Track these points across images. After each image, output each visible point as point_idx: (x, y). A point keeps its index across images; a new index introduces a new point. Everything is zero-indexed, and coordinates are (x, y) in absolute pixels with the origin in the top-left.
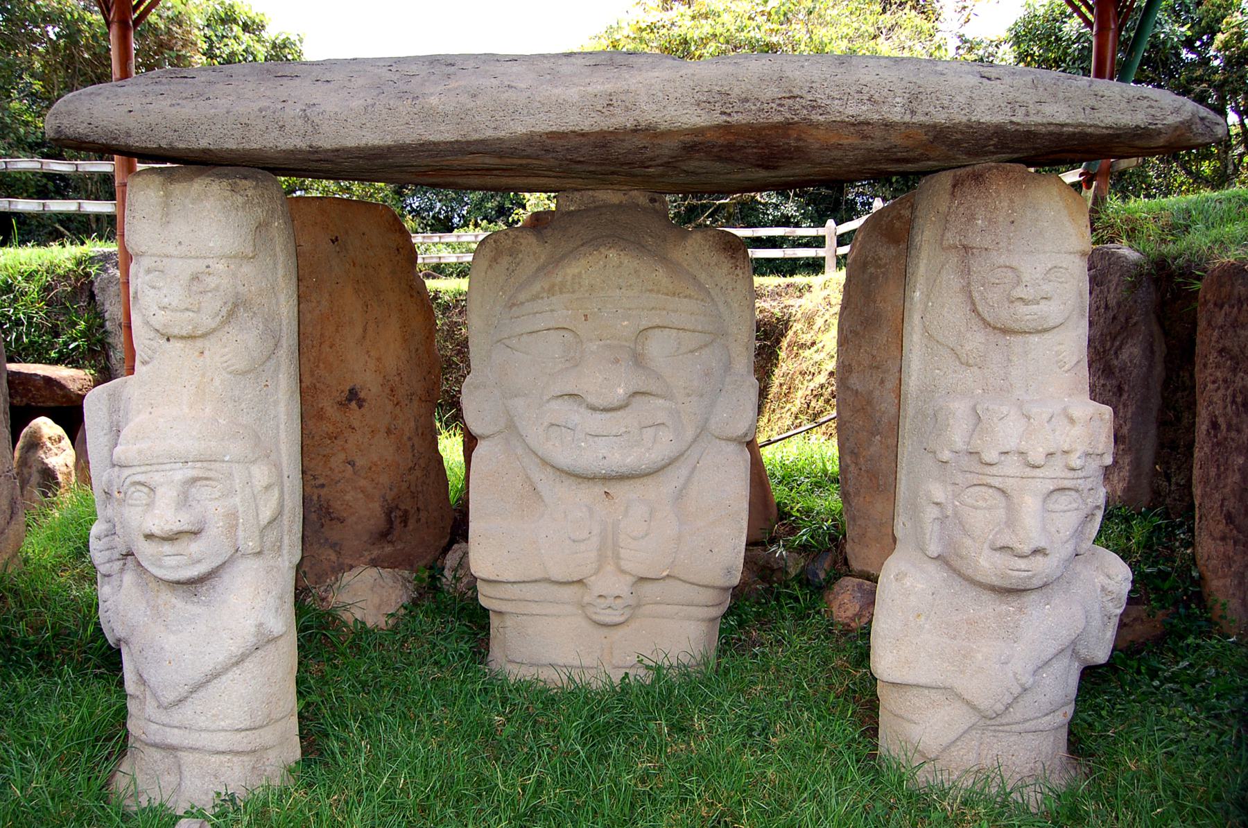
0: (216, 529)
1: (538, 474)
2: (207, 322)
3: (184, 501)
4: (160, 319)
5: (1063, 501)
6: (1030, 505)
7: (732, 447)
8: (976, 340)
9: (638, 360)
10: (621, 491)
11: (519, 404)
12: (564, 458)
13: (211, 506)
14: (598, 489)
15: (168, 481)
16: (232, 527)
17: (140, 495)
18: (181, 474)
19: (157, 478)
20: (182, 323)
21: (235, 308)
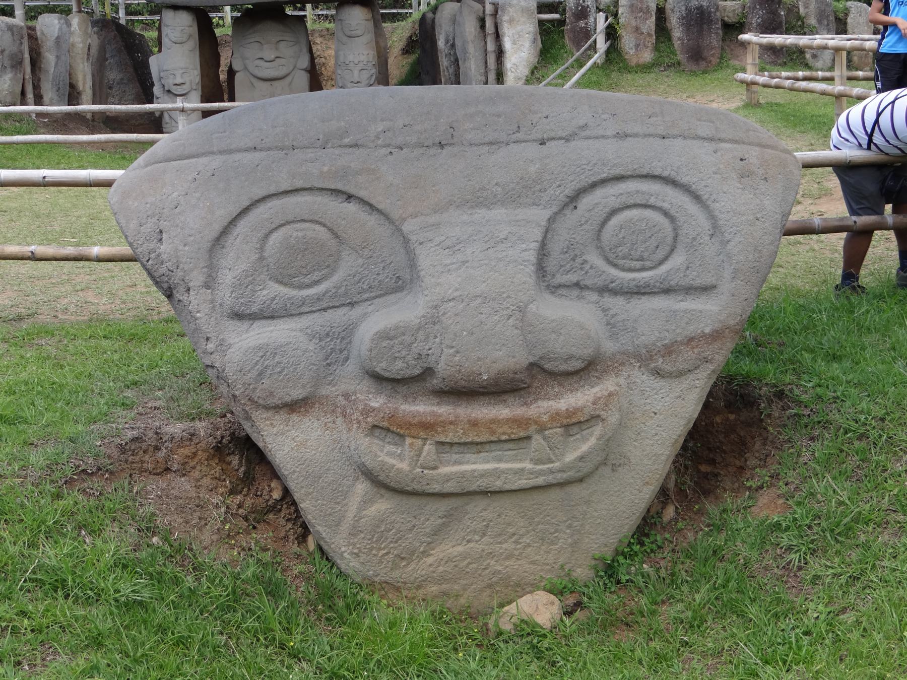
0: (188, 83)
1: (254, 80)
2: (185, 39)
3: (182, 77)
4: (174, 39)
5: (364, 72)
6: (356, 72)
7: (303, 72)
8: (345, 39)
9: (277, 49)
10: (275, 83)
11: (247, 61)
12: (260, 75)
13: (187, 79)
14: (269, 83)
15: (178, 73)
16: (191, 83)
17: (172, 76)
18: (181, 71)
19: (175, 72)
20: (180, 40)
21: (190, 36)
